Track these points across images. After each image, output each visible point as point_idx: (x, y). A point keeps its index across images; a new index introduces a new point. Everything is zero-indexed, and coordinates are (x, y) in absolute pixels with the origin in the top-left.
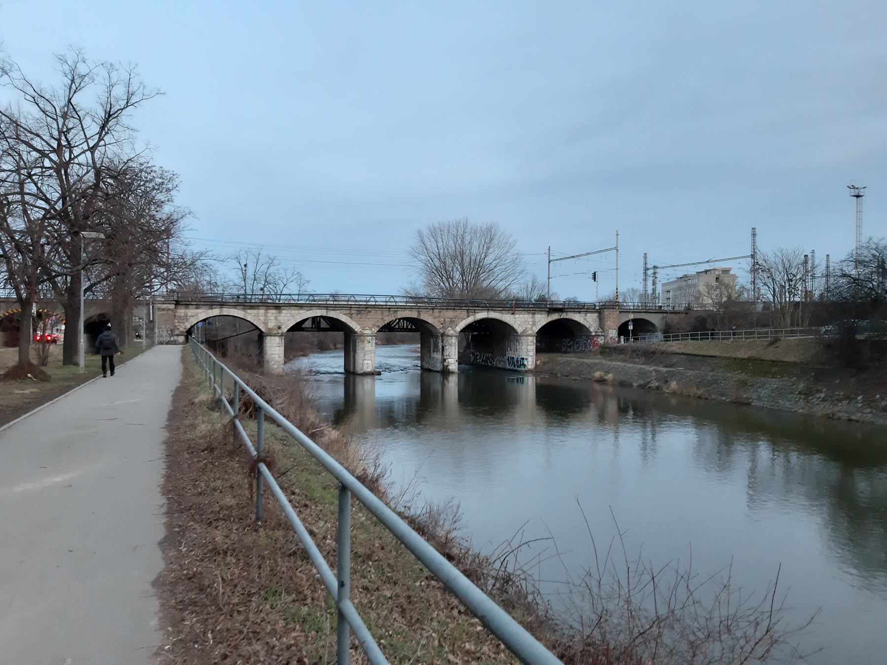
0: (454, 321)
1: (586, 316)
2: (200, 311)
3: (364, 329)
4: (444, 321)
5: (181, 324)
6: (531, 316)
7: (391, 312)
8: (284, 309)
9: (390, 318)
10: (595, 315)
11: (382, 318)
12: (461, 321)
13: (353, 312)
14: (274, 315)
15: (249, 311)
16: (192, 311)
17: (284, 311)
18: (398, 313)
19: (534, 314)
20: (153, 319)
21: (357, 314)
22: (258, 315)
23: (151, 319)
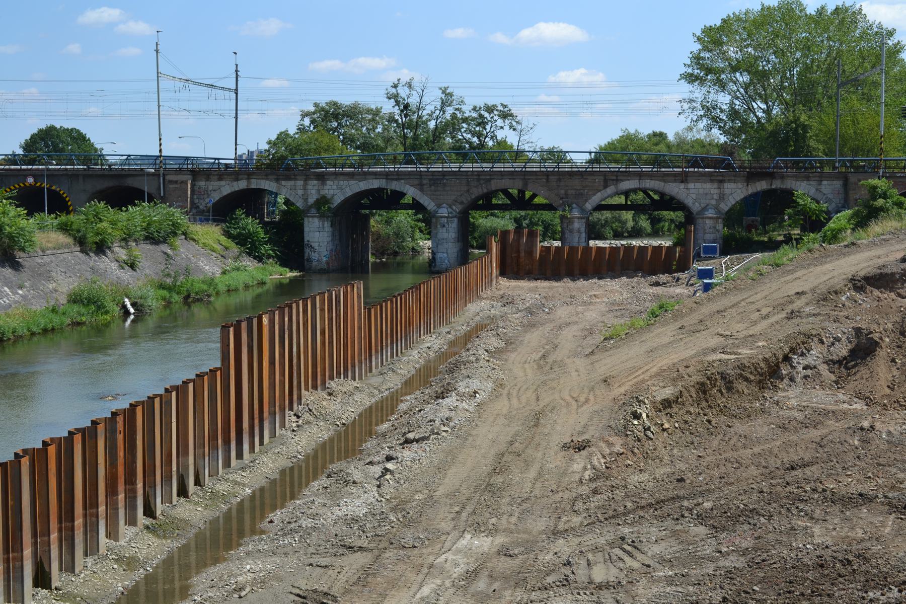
0: (582, 194)
1: (820, 184)
2: (223, 183)
3: (439, 206)
4: (566, 194)
5: (201, 201)
6: (716, 185)
7: (482, 182)
8: (328, 179)
9: (480, 190)
10: (838, 184)
11: (468, 191)
12: (594, 195)
13: (425, 182)
14: (316, 188)
15: (283, 183)
16: (214, 184)
17: (329, 183)
18: (492, 182)
19: (721, 182)
20: (164, 194)
21: (430, 186)
22: (294, 188)
23: (162, 194)
